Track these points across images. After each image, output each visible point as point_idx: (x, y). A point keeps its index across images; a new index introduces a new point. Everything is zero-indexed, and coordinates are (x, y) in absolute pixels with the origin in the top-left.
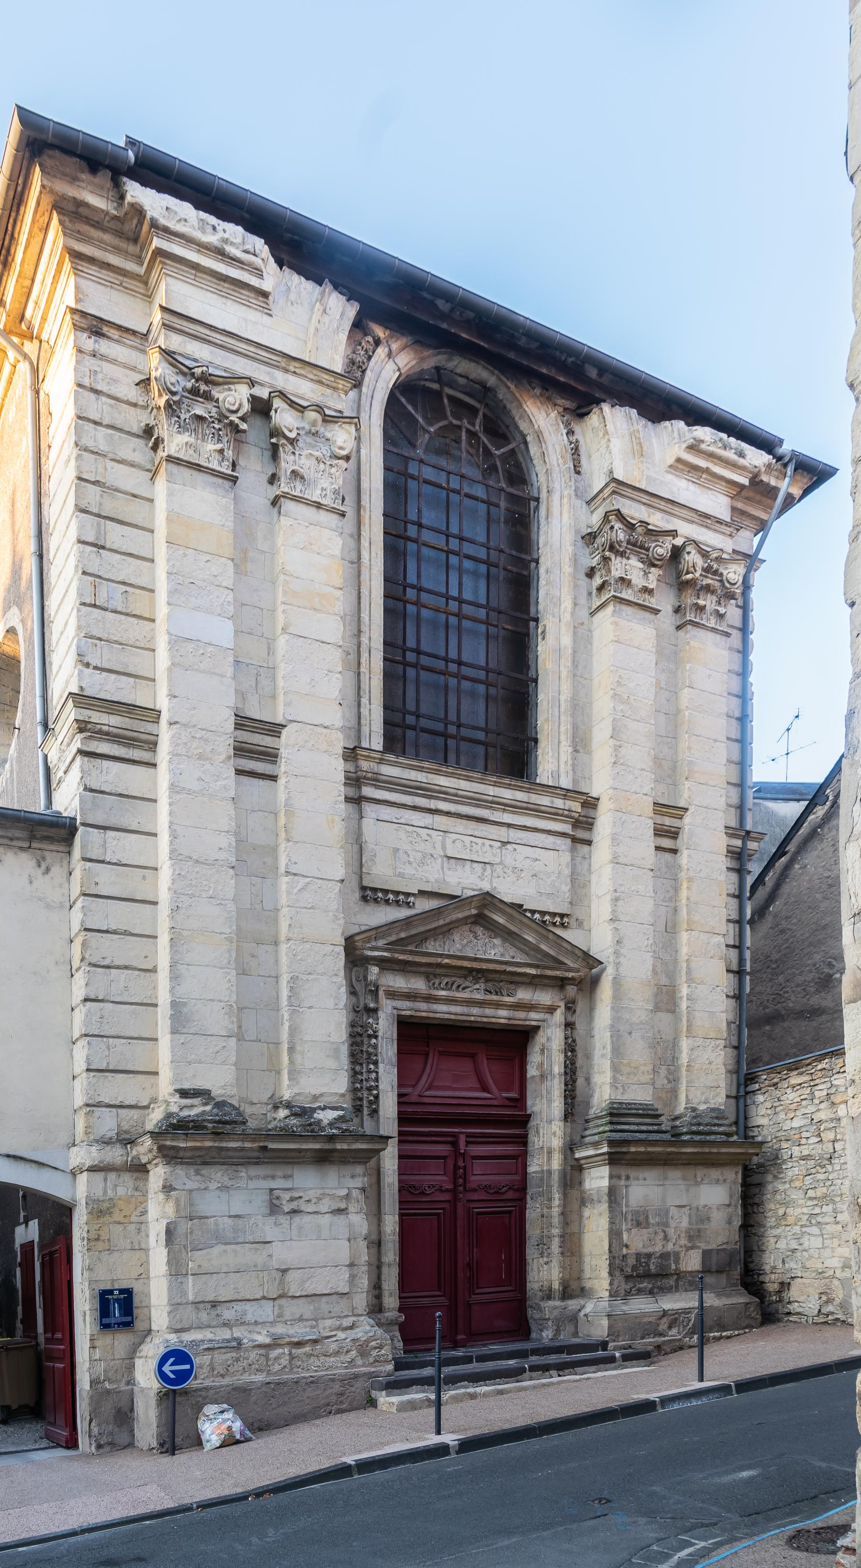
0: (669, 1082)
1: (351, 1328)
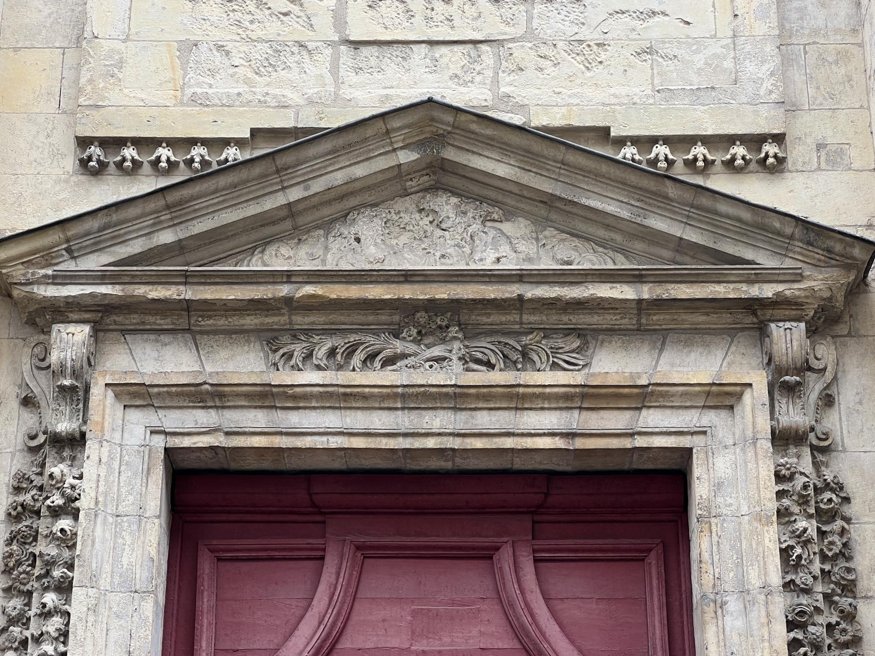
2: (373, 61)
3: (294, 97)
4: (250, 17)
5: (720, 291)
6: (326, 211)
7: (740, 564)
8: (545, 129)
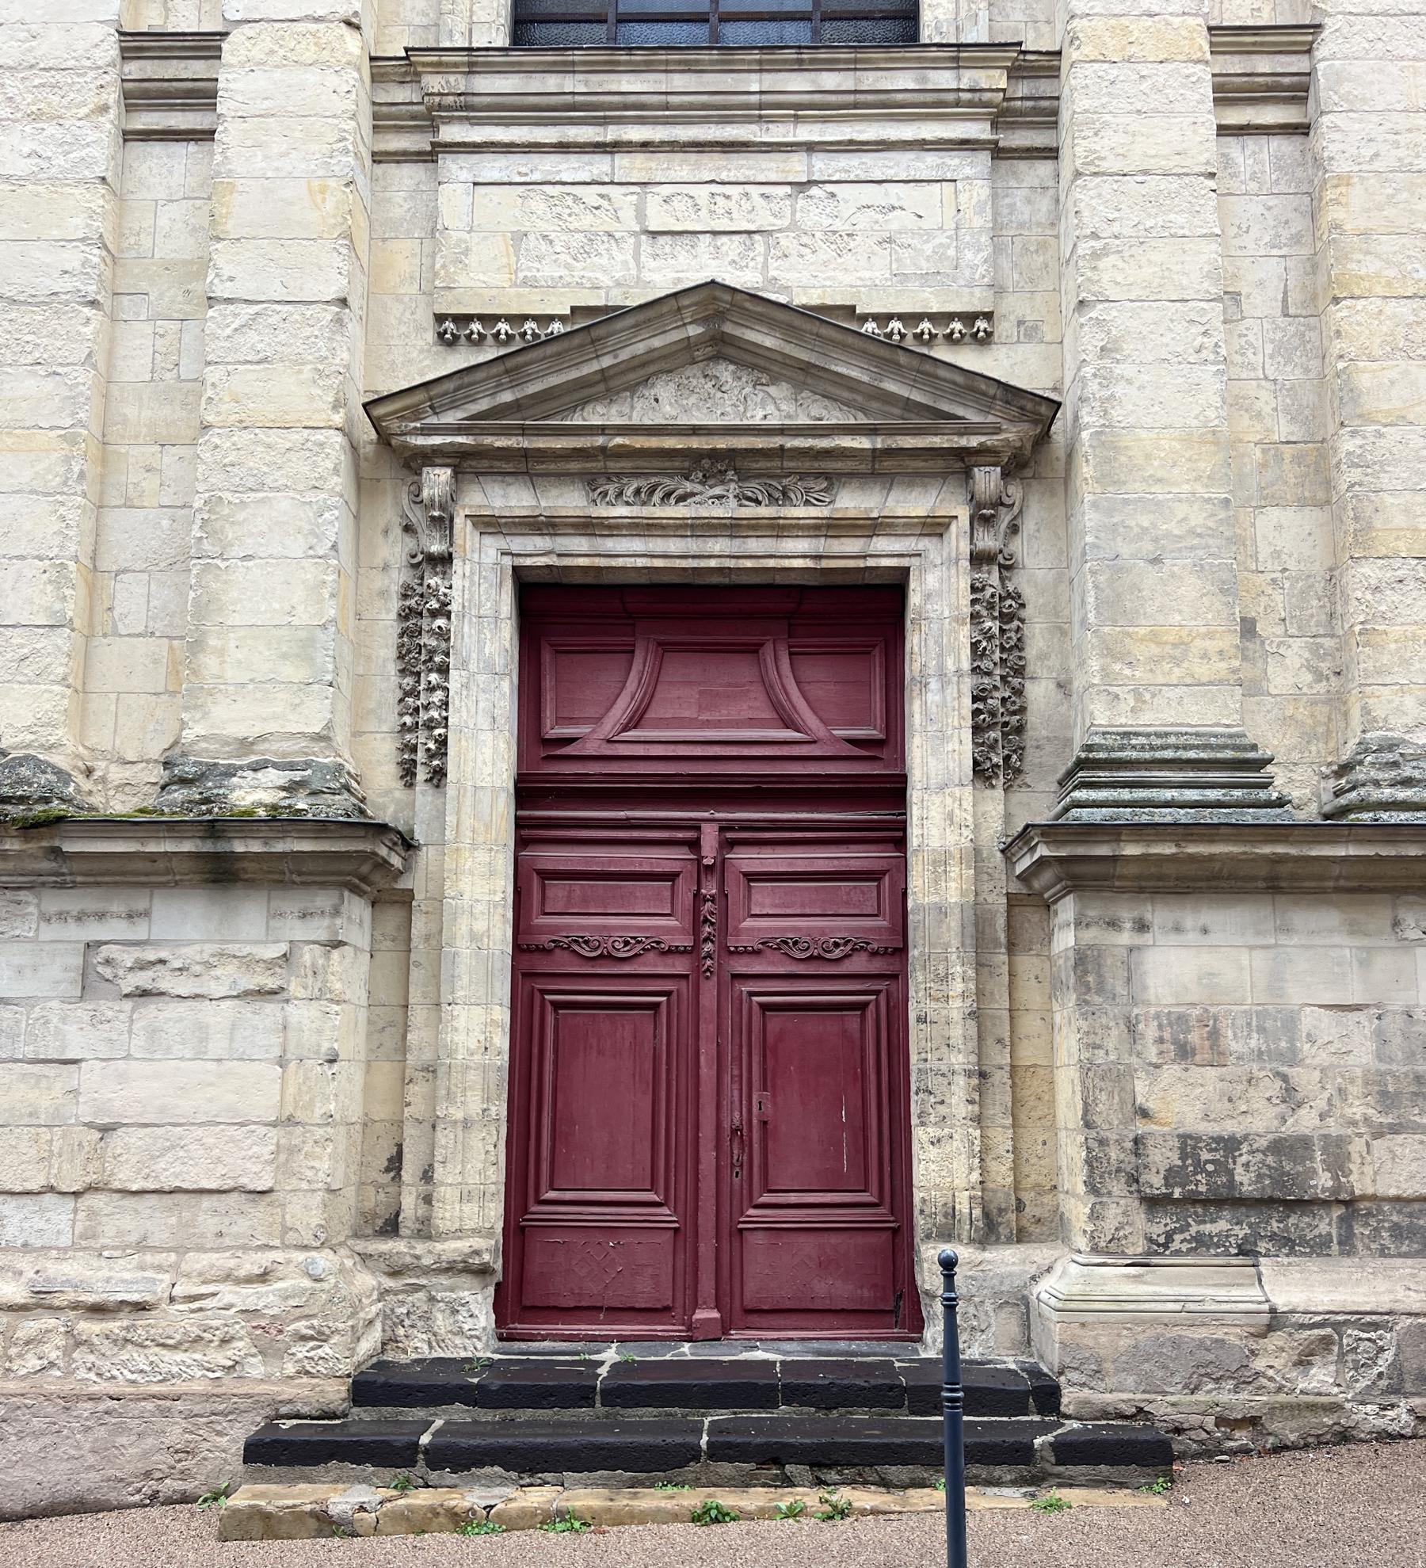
2: (668, 249)
3: (605, 280)
4: (568, 211)
5: (937, 441)
6: (632, 376)
7: (941, 655)
8: (804, 307)
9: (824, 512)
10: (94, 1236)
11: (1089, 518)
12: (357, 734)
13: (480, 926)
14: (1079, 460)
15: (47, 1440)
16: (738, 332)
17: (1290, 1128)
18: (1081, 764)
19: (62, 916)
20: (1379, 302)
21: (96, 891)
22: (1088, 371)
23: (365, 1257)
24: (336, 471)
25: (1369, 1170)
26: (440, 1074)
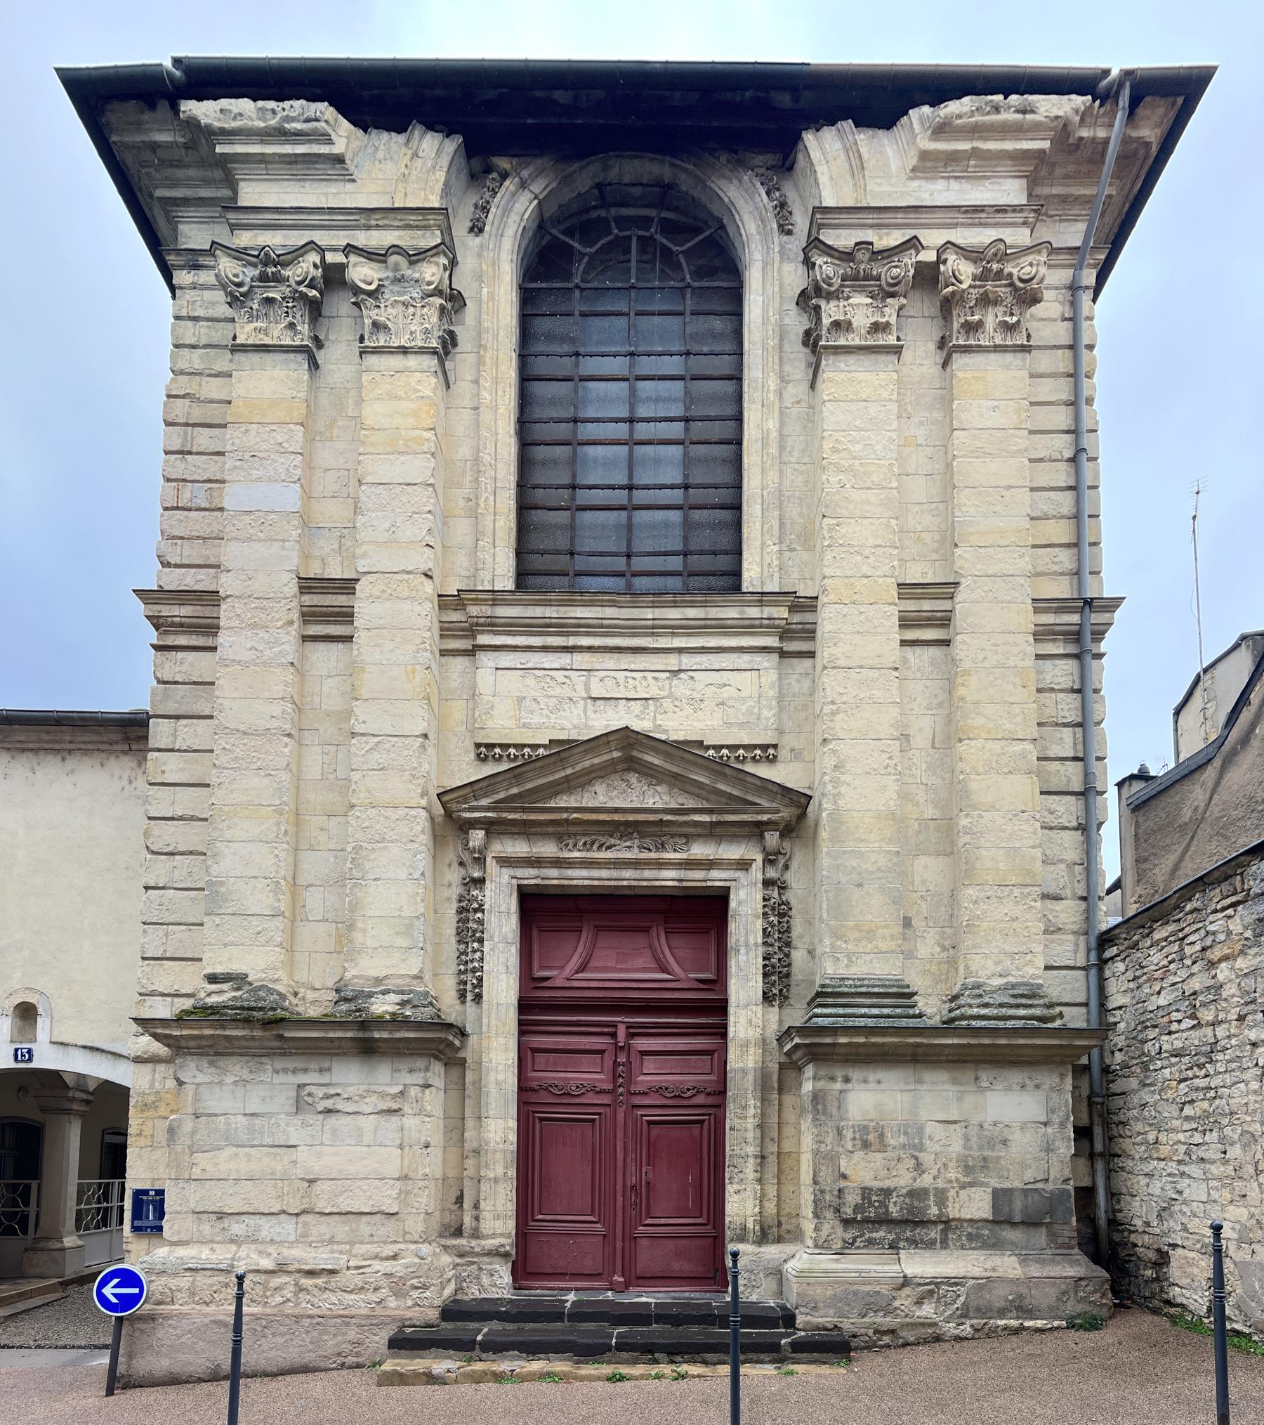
0: (944, 949)
1: (395, 1257)
3: (568, 725)
5: (745, 817)
6: (582, 779)
7: (746, 935)
9: (684, 856)
10: (307, 1236)
11: (825, 861)
12: (435, 975)
13: (501, 1077)
14: (821, 828)
15: (288, 1337)
16: (640, 755)
17: (918, 1184)
18: (819, 994)
19: (285, 1071)
20: (983, 742)
21: (302, 1058)
22: (827, 778)
23: (445, 1247)
24: (423, 832)
25: (957, 1205)
26: (483, 1152)
